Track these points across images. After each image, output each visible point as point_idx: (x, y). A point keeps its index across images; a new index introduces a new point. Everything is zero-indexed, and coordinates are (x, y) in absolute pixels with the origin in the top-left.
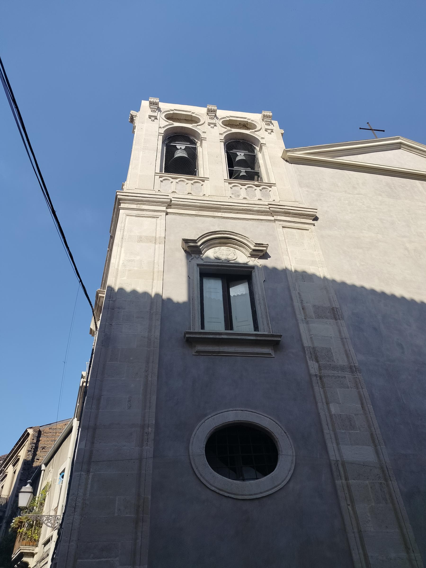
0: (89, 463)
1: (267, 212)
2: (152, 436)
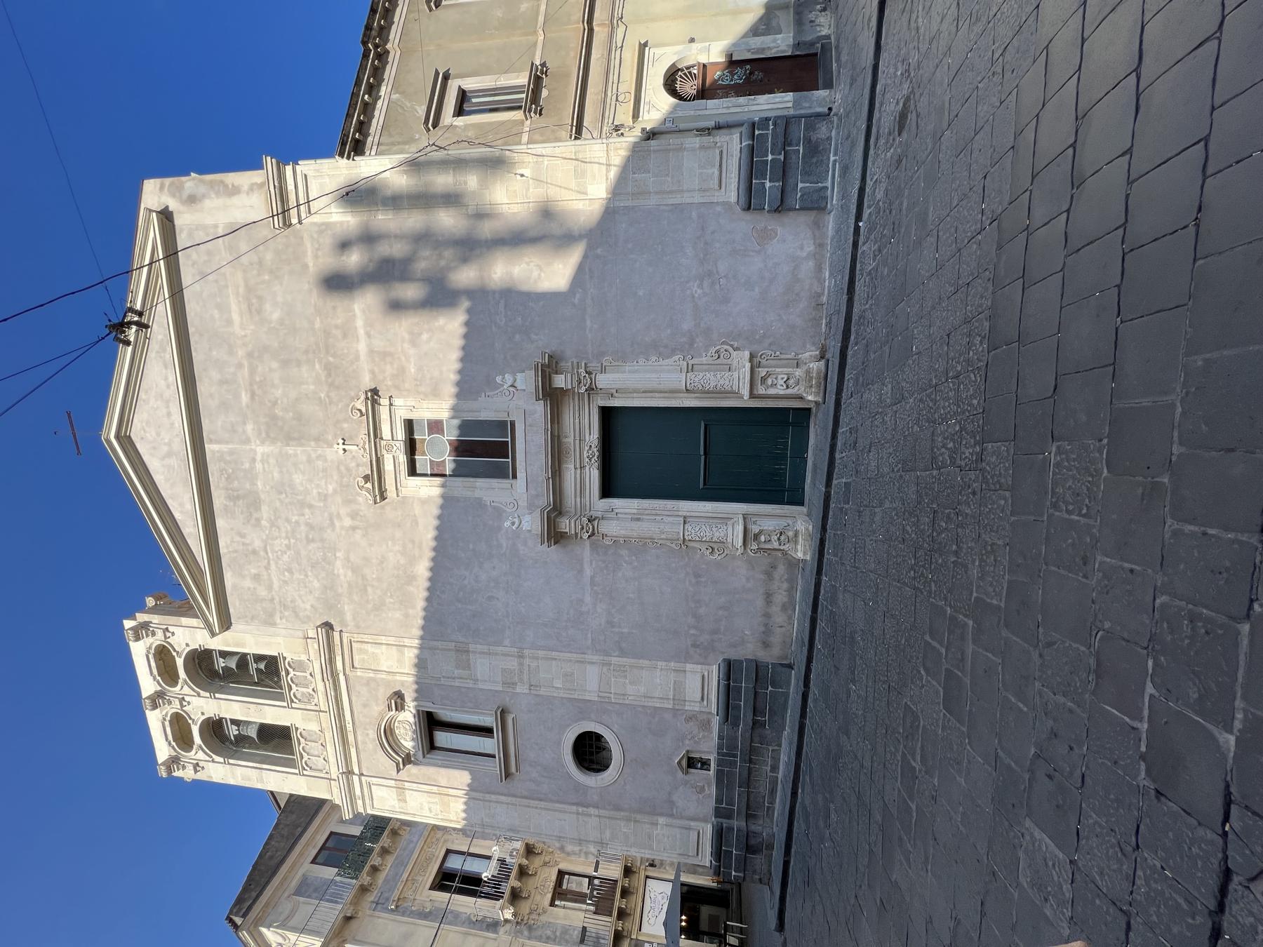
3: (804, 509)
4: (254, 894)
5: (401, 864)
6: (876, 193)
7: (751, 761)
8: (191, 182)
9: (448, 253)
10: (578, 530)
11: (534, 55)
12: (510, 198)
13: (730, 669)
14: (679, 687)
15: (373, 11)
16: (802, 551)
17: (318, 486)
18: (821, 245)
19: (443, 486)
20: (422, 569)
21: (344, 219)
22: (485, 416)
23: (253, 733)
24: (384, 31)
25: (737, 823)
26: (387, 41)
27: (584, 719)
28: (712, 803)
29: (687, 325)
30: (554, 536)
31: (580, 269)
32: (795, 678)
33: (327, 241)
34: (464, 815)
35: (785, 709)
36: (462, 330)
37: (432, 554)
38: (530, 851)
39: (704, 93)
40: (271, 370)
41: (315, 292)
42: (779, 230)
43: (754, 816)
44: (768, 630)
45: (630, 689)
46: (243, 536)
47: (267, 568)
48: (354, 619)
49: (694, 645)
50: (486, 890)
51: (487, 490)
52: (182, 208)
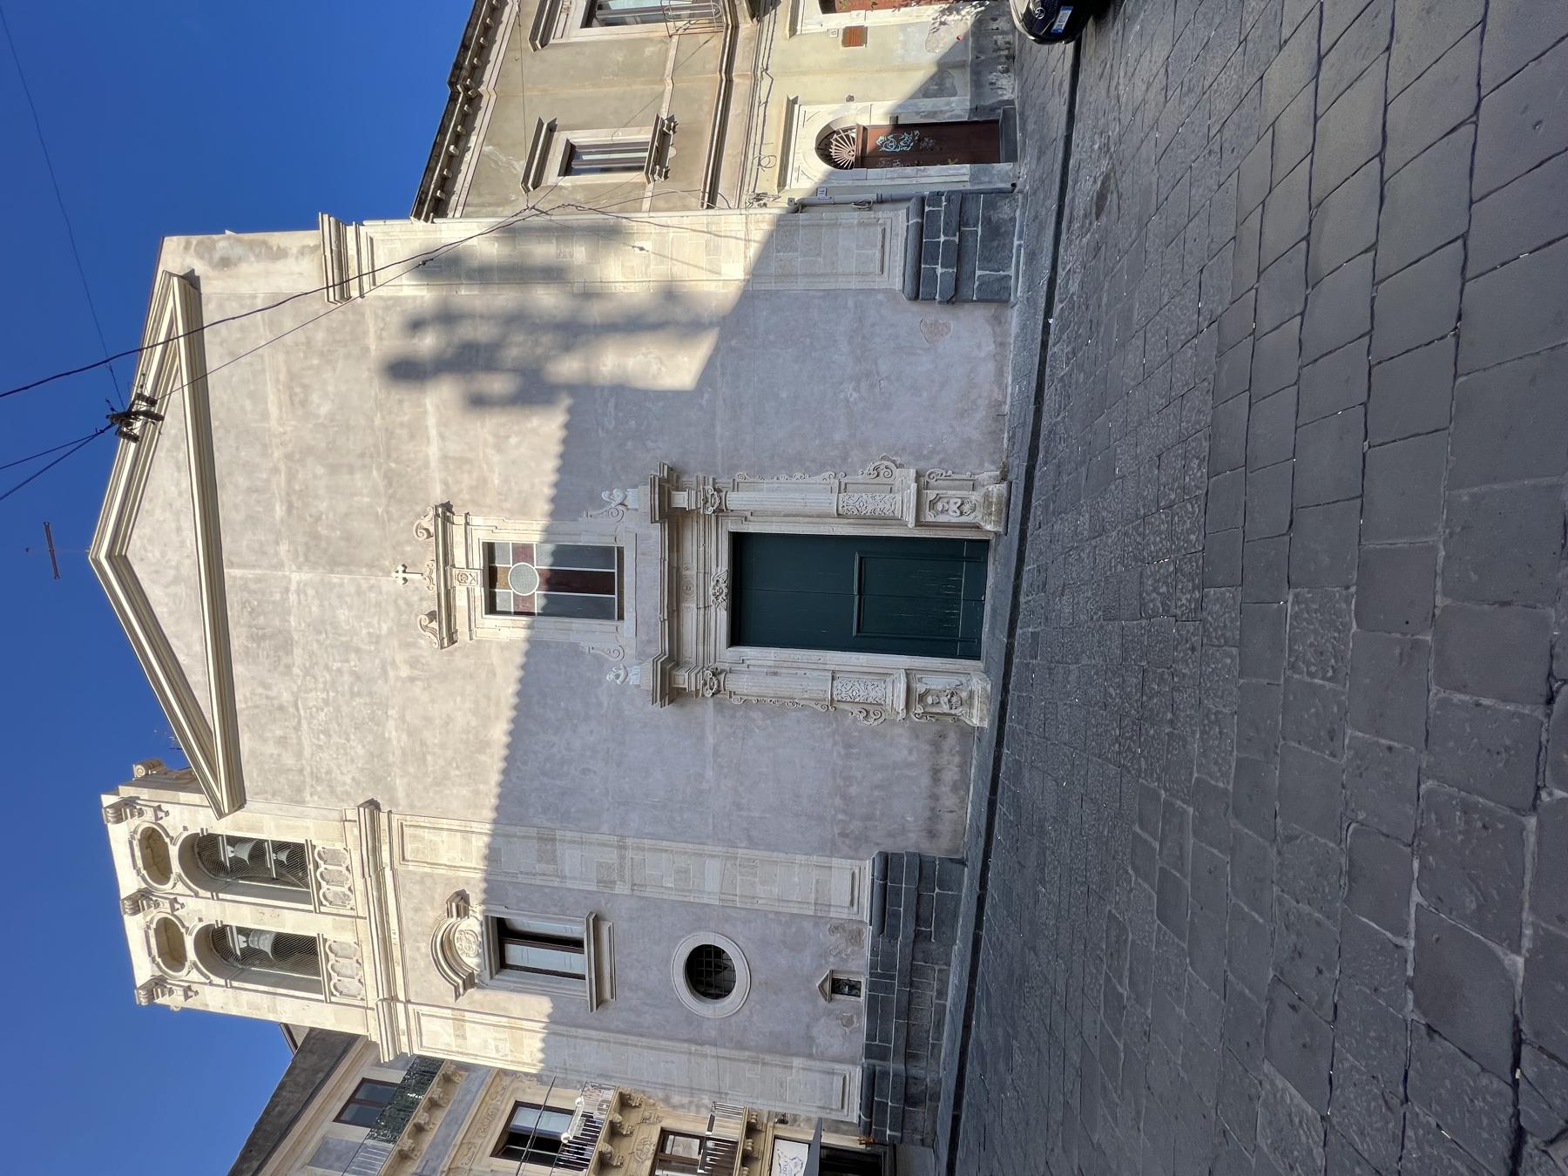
3: (980, 664)
4: (255, 1164)
5: (454, 1121)
7: (911, 984)
8: (225, 242)
9: (546, 339)
10: (700, 687)
12: (626, 275)
13: (888, 865)
15: (465, 46)
16: (978, 717)
18: (1002, 345)
19: (530, 627)
20: (499, 733)
22: (584, 540)
23: (266, 945)
24: (477, 72)
25: (894, 1066)
26: (480, 83)
27: (700, 929)
29: (837, 437)
30: (670, 693)
33: (395, 320)
34: (541, 1056)
35: (955, 917)
36: (560, 434)
37: (512, 714)
38: (624, 1103)
39: (863, 161)
40: (315, 477)
41: (376, 383)
42: (952, 324)
43: (915, 1057)
44: (934, 816)
46: (267, 687)
47: (297, 728)
48: (408, 796)
49: (843, 835)
50: (565, 1156)
51: (586, 633)
52: (211, 273)
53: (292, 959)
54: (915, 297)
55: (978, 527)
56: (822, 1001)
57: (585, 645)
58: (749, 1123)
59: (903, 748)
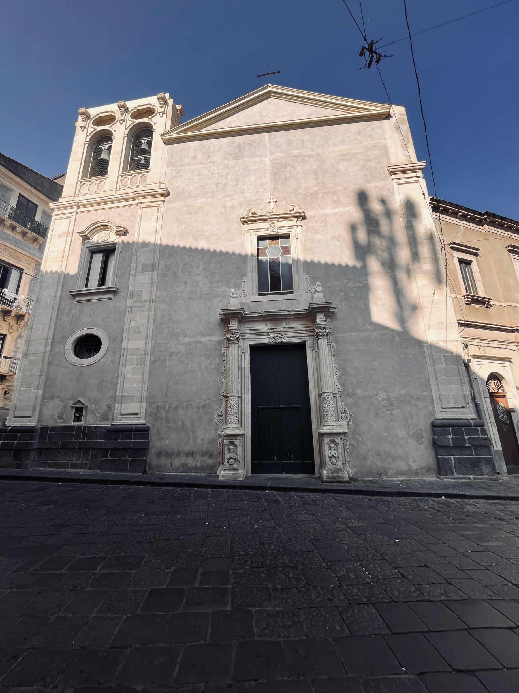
0: (26, 355)
1: (135, 198)
2: (50, 343)
3: (249, 474)
4: (3, 163)
5: (16, 243)
6: (470, 506)
7: (79, 449)
8: (406, 127)
9: (386, 255)
11: (495, 301)
12: (420, 287)
13: (142, 432)
14: (131, 399)
15: (502, 218)
16: (224, 474)
17: (248, 189)
20: (202, 244)
21: (397, 203)
22: (295, 277)
23: (103, 156)
24: (492, 224)
25: (36, 443)
27: (110, 340)
28: (51, 425)
29: (358, 391)
30: (226, 318)
31: (385, 328)
32: (137, 475)
33: (384, 193)
34: (49, 271)
35: (116, 470)
36: (343, 264)
37: (212, 250)
38: (20, 317)
39: (492, 396)
40: (312, 165)
41: (356, 187)
43: (40, 454)
44: (169, 455)
45: (129, 368)
46: (218, 151)
47: (200, 163)
48: (172, 208)
49: (158, 408)
51: (251, 280)
53: (97, 168)
54: (434, 425)
55: (322, 465)
56: (72, 402)
57: (246, 279)
58: (6, 376)
59: (204, 436)
